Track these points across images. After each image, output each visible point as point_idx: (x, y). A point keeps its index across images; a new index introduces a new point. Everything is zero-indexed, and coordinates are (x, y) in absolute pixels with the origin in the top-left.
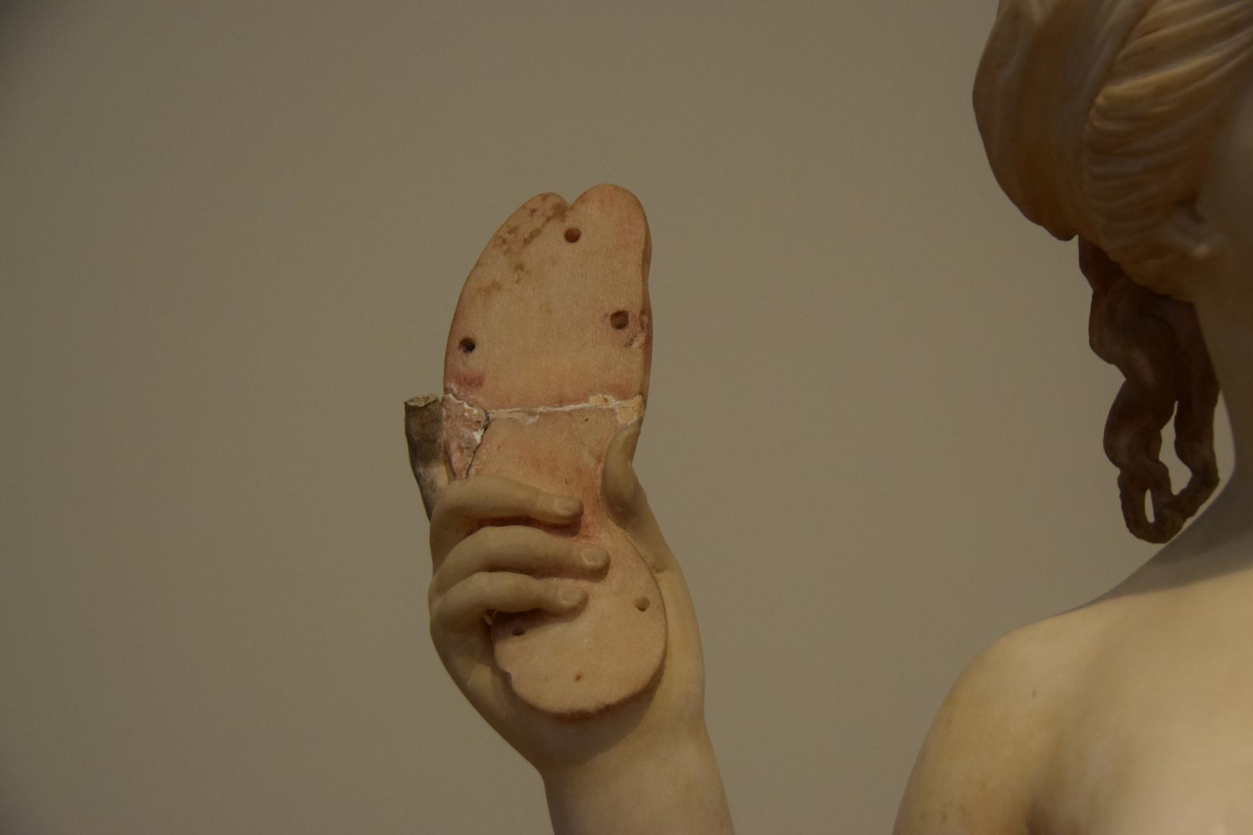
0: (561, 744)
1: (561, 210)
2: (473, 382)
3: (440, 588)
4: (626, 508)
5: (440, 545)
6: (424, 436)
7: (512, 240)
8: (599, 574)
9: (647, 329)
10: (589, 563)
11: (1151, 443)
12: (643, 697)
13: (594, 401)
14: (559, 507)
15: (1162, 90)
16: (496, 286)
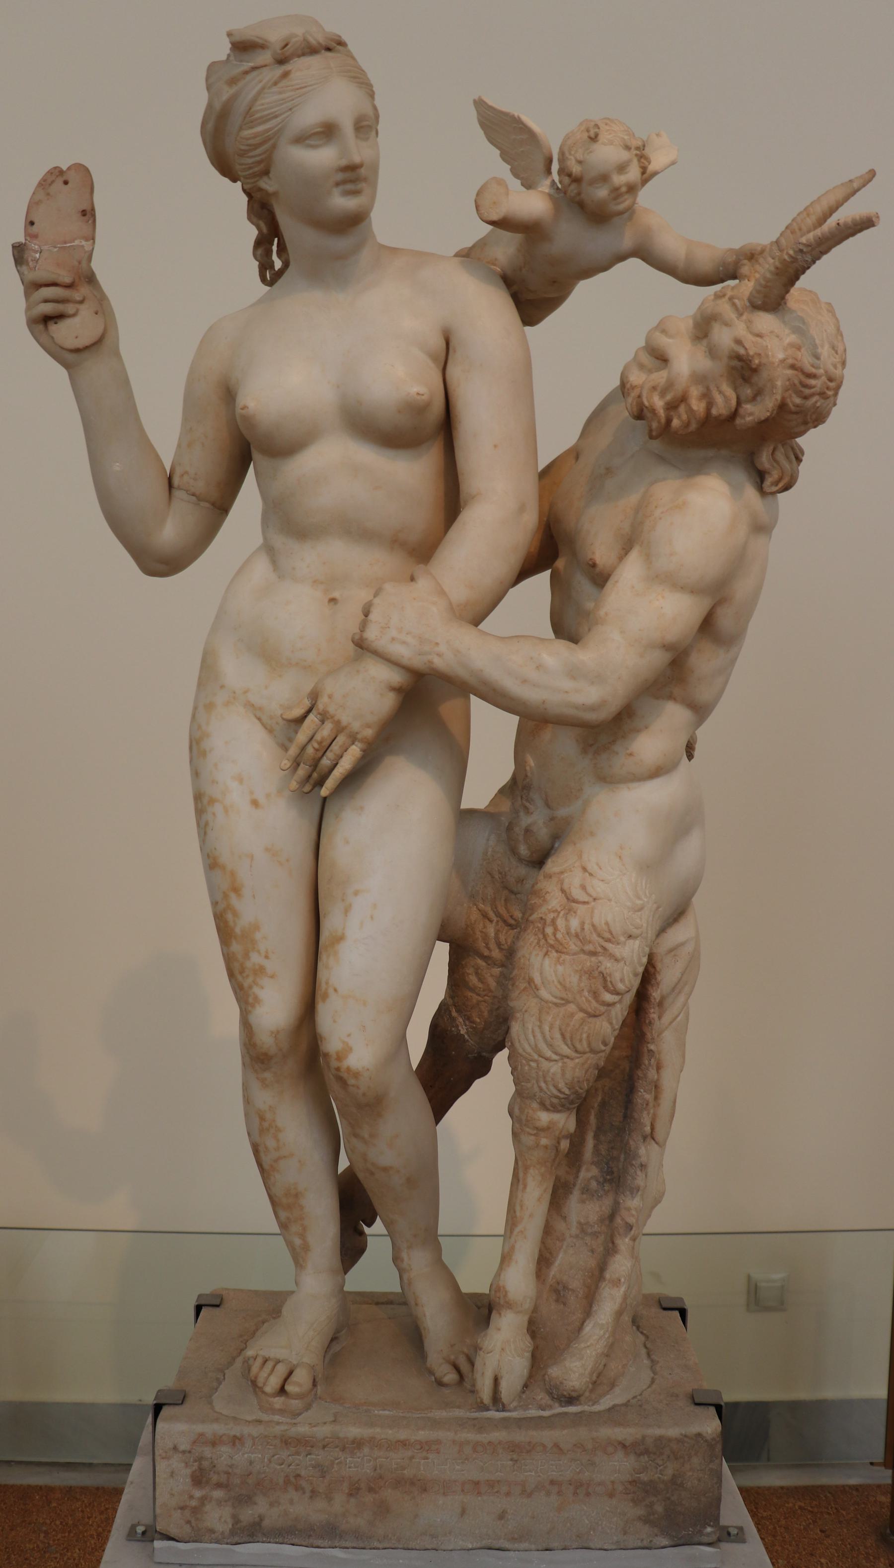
0: (72, 358)
1: (61, 172)
6: (20, 253)
11: (269, 253)
12: (98, 342)
15: (255, 136)
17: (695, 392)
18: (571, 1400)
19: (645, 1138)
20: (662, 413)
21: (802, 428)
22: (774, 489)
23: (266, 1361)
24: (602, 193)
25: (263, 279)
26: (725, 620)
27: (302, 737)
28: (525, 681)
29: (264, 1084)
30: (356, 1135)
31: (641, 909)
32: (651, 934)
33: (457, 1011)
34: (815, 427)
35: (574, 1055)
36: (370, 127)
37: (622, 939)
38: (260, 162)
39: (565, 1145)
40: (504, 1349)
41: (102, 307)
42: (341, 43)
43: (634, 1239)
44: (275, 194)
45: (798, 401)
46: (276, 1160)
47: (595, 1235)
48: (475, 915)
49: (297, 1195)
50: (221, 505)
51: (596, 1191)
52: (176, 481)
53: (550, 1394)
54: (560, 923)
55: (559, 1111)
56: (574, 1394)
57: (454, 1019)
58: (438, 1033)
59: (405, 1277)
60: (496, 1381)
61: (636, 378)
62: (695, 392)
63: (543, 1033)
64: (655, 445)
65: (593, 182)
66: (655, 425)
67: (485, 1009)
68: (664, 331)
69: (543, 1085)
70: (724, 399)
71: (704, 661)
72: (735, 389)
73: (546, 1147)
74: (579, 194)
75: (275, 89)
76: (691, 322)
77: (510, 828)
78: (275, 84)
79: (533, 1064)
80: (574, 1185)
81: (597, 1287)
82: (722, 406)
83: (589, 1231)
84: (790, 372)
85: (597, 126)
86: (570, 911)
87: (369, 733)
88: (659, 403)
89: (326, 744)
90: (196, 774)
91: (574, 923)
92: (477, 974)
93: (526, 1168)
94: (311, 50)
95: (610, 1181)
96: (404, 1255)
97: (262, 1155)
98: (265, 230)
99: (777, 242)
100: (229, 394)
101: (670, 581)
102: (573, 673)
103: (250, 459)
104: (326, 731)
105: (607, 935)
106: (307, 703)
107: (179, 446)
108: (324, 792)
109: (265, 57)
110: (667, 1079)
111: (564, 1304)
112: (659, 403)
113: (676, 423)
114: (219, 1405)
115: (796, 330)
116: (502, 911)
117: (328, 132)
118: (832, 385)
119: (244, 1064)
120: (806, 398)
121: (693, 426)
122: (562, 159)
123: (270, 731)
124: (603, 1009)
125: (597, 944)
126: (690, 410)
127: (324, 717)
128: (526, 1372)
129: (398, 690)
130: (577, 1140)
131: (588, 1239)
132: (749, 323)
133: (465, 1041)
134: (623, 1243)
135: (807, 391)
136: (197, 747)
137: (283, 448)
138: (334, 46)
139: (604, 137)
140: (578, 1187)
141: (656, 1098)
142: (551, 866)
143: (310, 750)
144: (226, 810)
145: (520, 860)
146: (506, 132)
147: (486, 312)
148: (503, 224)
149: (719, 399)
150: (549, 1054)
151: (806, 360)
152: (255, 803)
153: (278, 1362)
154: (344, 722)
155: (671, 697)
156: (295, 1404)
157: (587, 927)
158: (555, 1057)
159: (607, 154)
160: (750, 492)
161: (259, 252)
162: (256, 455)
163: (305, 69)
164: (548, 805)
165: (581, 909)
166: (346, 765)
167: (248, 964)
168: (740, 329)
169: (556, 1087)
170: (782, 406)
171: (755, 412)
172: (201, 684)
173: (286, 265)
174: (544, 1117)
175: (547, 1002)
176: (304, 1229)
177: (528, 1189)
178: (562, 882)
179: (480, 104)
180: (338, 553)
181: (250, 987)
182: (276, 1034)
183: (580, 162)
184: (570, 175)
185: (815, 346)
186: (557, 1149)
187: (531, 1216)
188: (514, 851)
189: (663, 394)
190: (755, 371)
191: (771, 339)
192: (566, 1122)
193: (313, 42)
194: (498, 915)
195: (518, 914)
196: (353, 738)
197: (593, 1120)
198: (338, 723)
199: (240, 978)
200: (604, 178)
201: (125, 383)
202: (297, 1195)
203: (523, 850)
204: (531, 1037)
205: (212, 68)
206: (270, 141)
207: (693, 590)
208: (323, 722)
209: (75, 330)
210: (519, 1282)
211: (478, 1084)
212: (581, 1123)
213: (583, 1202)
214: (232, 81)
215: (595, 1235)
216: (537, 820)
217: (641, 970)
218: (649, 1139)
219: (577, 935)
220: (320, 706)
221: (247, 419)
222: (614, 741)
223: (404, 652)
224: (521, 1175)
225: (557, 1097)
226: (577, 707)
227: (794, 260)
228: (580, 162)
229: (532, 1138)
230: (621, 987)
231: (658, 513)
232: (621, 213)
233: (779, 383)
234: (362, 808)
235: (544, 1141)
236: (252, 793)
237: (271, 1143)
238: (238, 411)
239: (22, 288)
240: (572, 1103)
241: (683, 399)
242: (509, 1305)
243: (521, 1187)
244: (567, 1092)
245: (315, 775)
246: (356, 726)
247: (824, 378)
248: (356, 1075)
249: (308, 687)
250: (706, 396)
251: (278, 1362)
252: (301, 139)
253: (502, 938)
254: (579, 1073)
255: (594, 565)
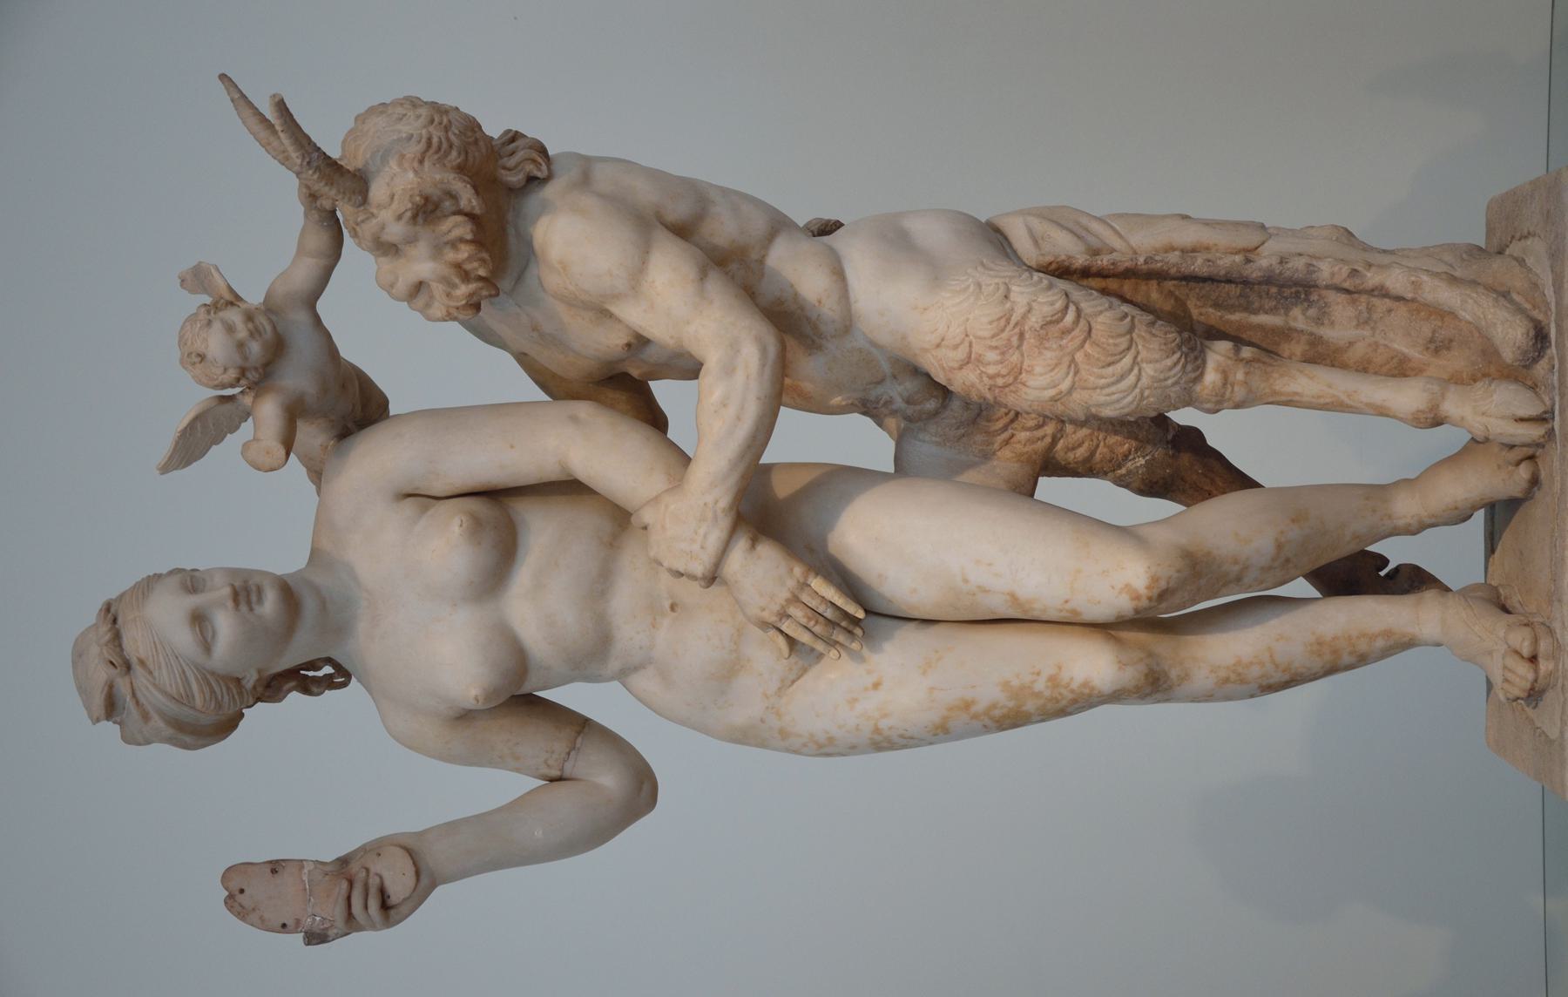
0: (425, 880)
1: (231, 896)
2: (298, 922)
3: (373, 927)
4: (344, 861)
5: (360, 928)
6: (315, 938)
7: (242, 913)
8: (367, 870)
9: (277, 861)
10: (364, 874)
12: (410, 852)
13: (305, 878)
14: (345, 885)
16: (262, 918)
17: (451, 255)
18: (1540, 337)
19: (1248, 261)
20: (473, 286)
21: (481, 143)
22: (544, 167)
23: (1506, 680)
24: (255, 348)
25: (344, 685)
26: (679, 210)
27: (805, 638)
28: (739, 419)
29: (1185, 677)
30: (1238, 579)
31: (979, 285)
32: (1007, 269)
33: (1120, 467)
34: (480, 127)
35: (1133, 351)
36: (192, 578)
37: (1008, 305)
38: (228, 688)
39: (1247, 352)
40: (1495, 409)
41: (375, 849)
42: (108, 608)
43: (1370, 265)
44: (259, 671)
45: (454, 153)
46: (1277, 666)
47: (1370, 309)
48: (1007, 453)
49: (1320, 643)
50: (581, 725)
51: (1320, 309)
52: (555, 773)
53: (1535, 360)
54: (992, 370)
55: (1204, 362)
56: (1532, 333)
57: (1129, 472)
58: (1152, 487)
59: (1429, 521)
60: (1522, 420)
61: (438, 309)
62: (451, 255)
63: (1109, 385)
64: (505, 284)
65: (246, 358)
66: (485, 293)
67: (1112, 439)
68: (392, 286)
69: (1170, 382)
70: (457, 227)
71: (723, 229)
72: (446, 216)
73: (1247, 374)
74: (256, 369)
75: (156, 674)
76: (382, 259)
77: (909, 419)
78: (151, 673)
79: (1147, 393)
80: (1311, 334)
81: (1426, 305)
82: (463, 229)
83: (1365, 315)
84: (427, 164)
85: (189, 355)
86: (980, 360)
87: (798, 570)
88: (463, 290)
89: (810, 613)
90: (853, 749)
91: (992, 356)
92: (1073, 449)
93: (1275, 393)
94: (117, 637)
95: (1307, 294)
96: (1401, 523)
97: (1272, 681)
98: (292, 684)
99: (298, 174)
100: (464, 717)
101: (638, 272)
102: (729, 370)
103: (531, 695)
104: (797, 612)
105: (1003, 322)
106: (772, 632)
107: (518, 770)
108: (860, 614)
109: (123, 686)
110: (1188, 236)
111: (1451, 341)
112: (463, 290)
113: (482, 272)
114: (1554, 733)
115: (384, 160)
116: (1000, 424)
117: (199, 620)
118: (437, 120)
119: (1167, 700)
120: (451, 146)
121: (485, 255)
122: (224, 387)
123: (805, 670)
124: (1083, 322)
125: (1013, 331)
126: (469, 259)
127: (784, 615)
128: (1513, 387)
129: (754, 542)
130: (1237, 340)
131: (1375, 316)
132: (379, 207)
133: (1153, 459)
134: (1372, 278)
135: (445, 145)
136: (826, 748)
137: (518, 661)
138: (110, 614)
139: (202, 349)
140: (1315, 330)
141: (1208, 249)
142: (941, 378)
143: (818, 629)
144: (885, 716)
145: (944, 406)
146: (194, 442)
147: (378, 459)
148: (288, 445)
149: (457, 233)
150: (1132, 378)
151: (414, 149)
152: (876, 686)
153: (1505, 667)
154: (786, 595)
155: (761, 261)
156: (1544, 646)
157: (994, 343)
158: (1136, 371)
159: (216, 344)
160: (549, 191)
161: (315, 690)
162: (526, 689)
163: (136, 643)
164: (881, 382)
165: (976, 349)
166: (831, 593)
167: (1047, 693)
168: (386, 215)
169: (1171, 369)
170: (461, 169)
171: (468, 198)
172: (763, 744)
173: (329, 661)
174: (1211, 377)
175: (1074, 383)
176: (1364, 635)
177: (1299, 390)
178: (952, 369)
179: (165, 469)
180: (624, 601)
181: (1072, 691)
182: (1122, 665)
183: (226, 370)
184: (238, 380)
185: (399, 140)
186: (1248, 362)
187: (1330, 386)
188: (936, 413)
189: (454, 286)
190: (427, 199)
191: (395, 185)
192: (1218, 353)
193: (108, 637)
194: (1005, 428)
195: (1003, 410)
196: (804, 585)
197: (1236, 317)
198: (789, 601)
199: (1064, 702)
200: (241, 345)
201: (452, 827)
202: (1320, 643)
203: (931, 405)
204: (1115, 397)
205: (128, 739)
206: (209, 677)
207: (645, 251)
208: (789, 616)
209: (399, 884)
210: (1408, 397)
211: (1212, 441)
212: (1220, 335)
213: (1332, 323)
214: (146, 717)
215: (1370, 309)
216: (897, 391)
217: (1046, 280)
218: (1251, 256)
219: (1003, 353)
220: (773, 619)
221: (488, 698)
222: (808, 319)
223: (715, 537)
224: (1283, 398)
225: (1184, 367)
226: (763, 366)
227: (318, 169)
228: (226, 370)
229: (1236, 388)
230: (1059, 305)
231: (572, 288)
232: (274, 328)
233: (438, 177)
234: (880, 576)
235: (1240, 376)
236: (866, 689)
237: (1255, 672)
238: (480, 706)
239: (354, 935)
240: (1192, 349)
241: (458, 266)
242: (1434, 408)
243: (1297, 398)
244: (1177, 355)
245: (844, 624)
246: (791, 583)
247: (431, 129)
248: (1155, 579)
249: (757, 632)
250: (454, 244)
251: (1505, 667)
252: (207, 646)
253: (1031, 423)
254: (1155, 344)
255: (629, 345)
